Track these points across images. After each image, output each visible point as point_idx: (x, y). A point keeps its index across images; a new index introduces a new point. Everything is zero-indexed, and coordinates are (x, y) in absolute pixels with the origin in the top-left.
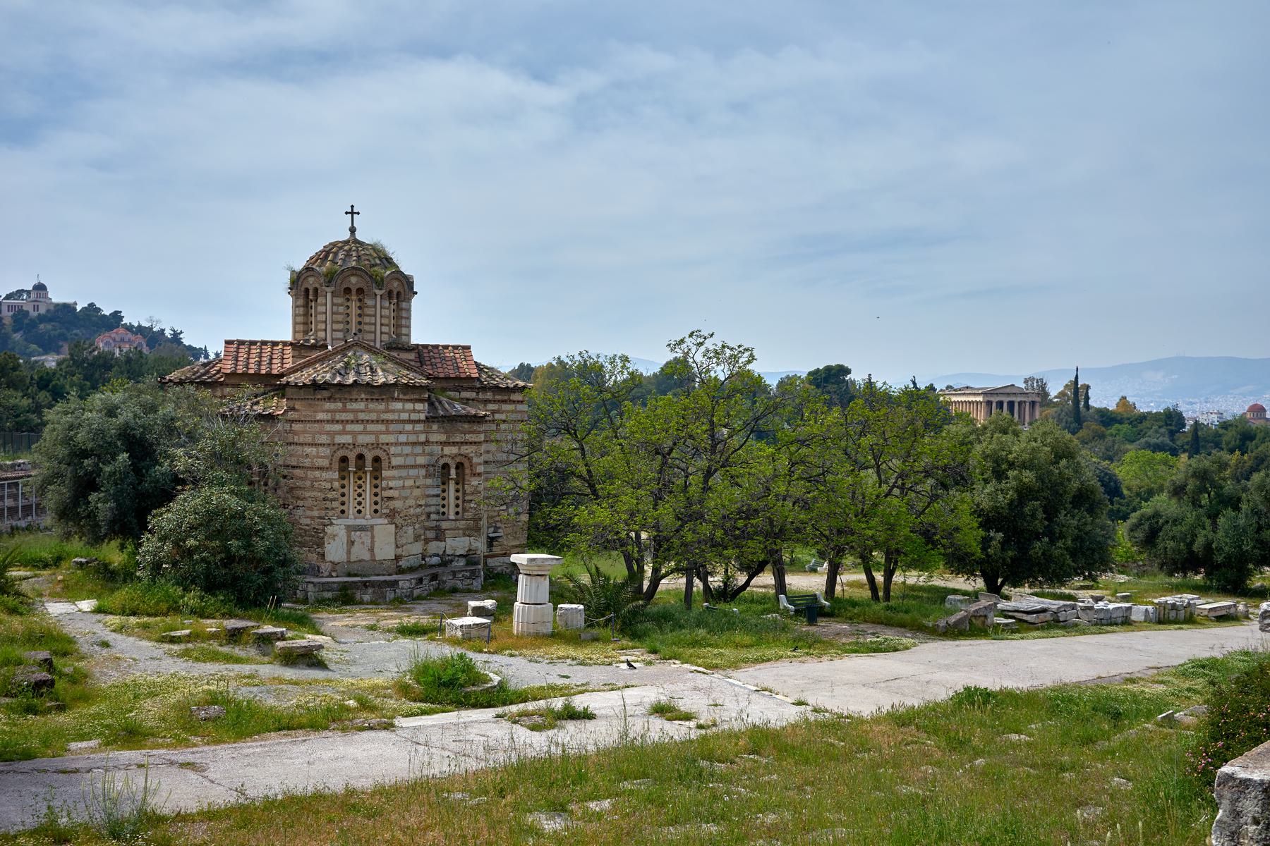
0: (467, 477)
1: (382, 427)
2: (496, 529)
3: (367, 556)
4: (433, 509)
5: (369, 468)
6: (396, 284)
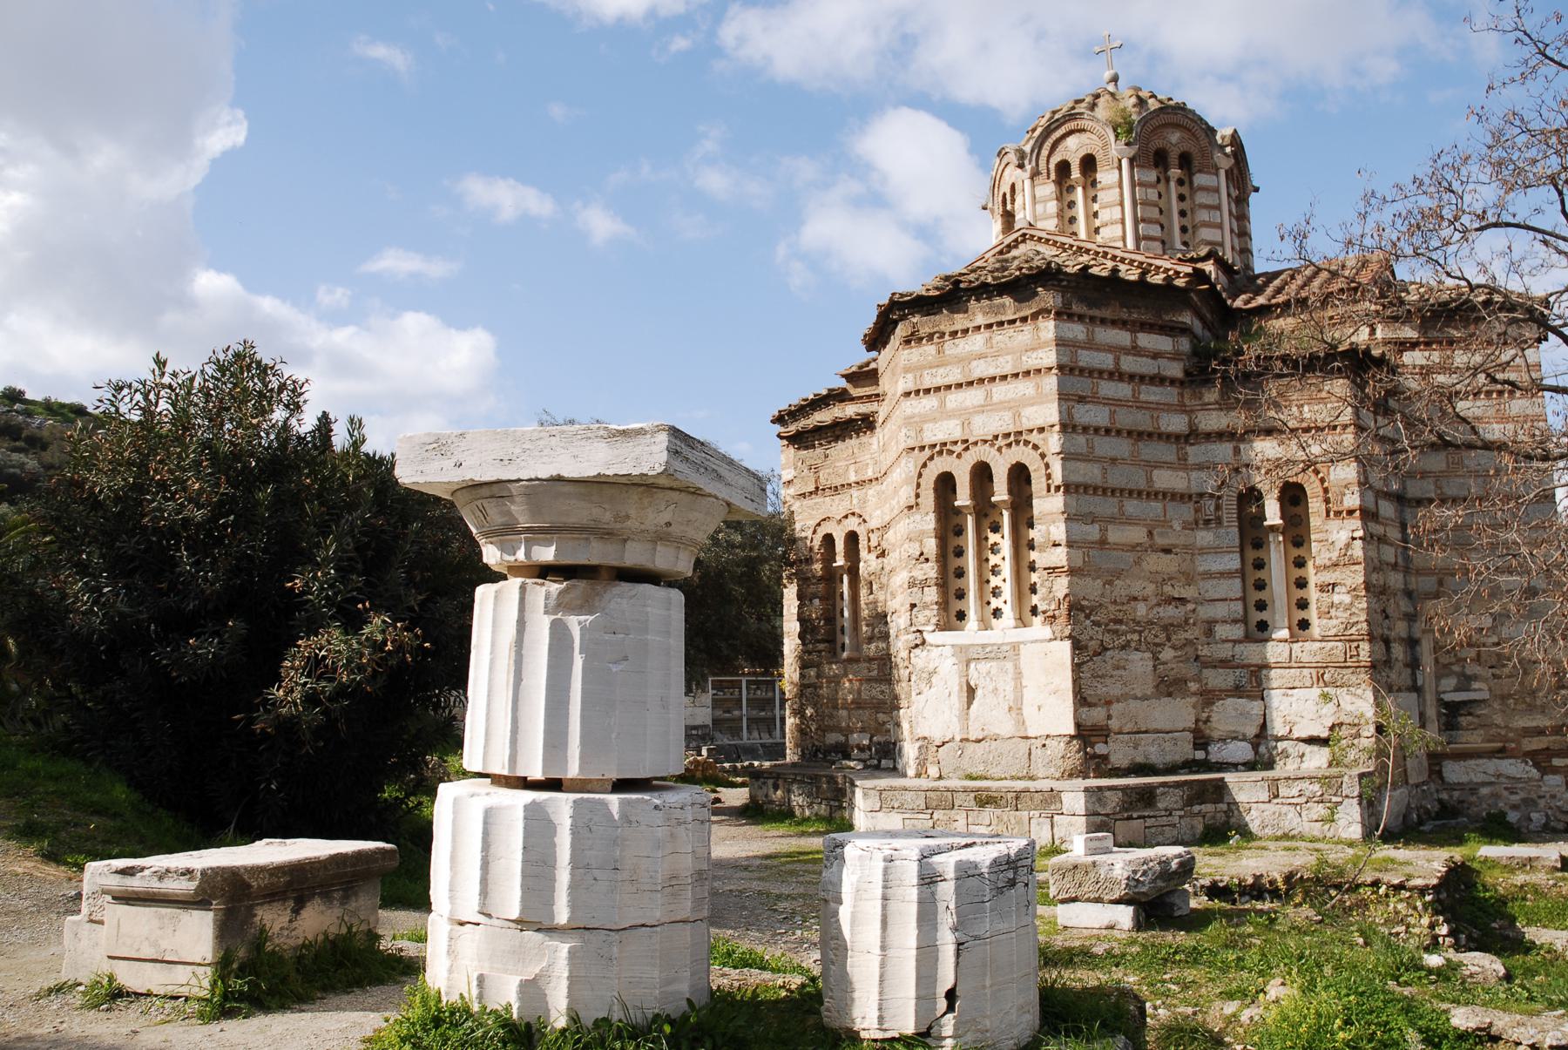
0: (1315, 521)
1: (1024, 387)
2: (1465, 682)
3: (1005, 727)
4: (1220, 611)
5: (1001, 493)
6: (1175, 137)
